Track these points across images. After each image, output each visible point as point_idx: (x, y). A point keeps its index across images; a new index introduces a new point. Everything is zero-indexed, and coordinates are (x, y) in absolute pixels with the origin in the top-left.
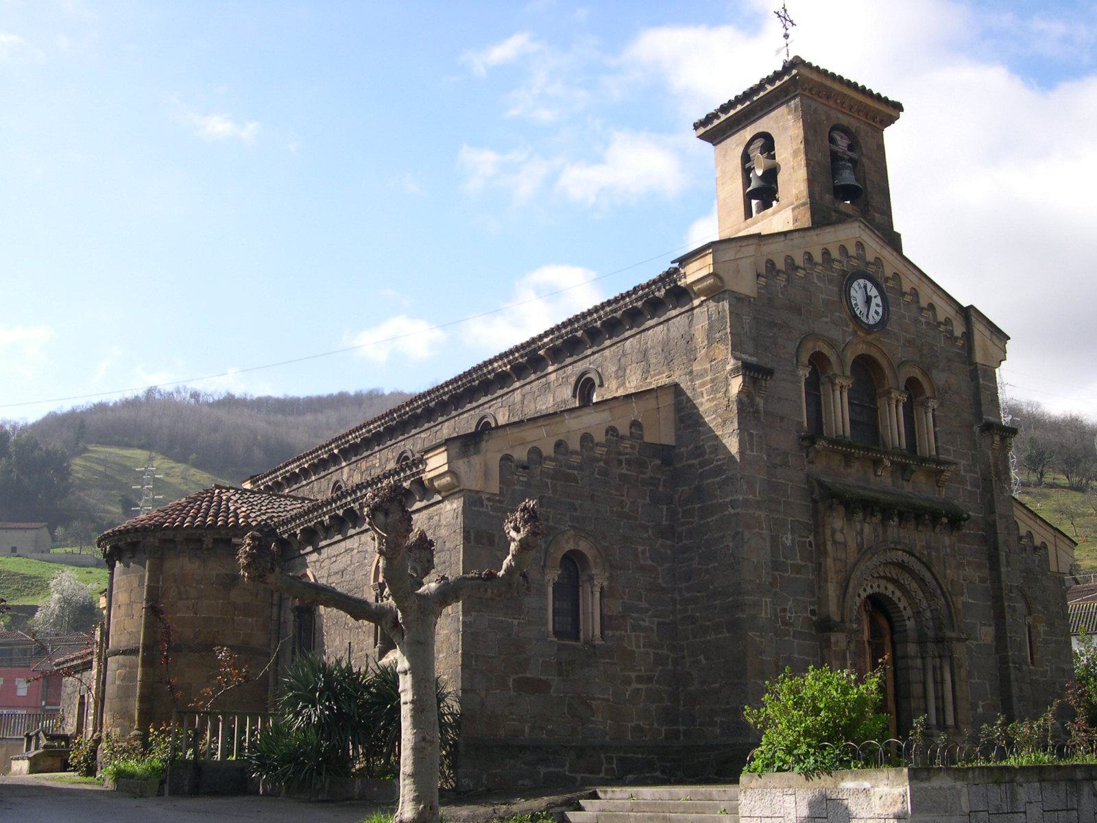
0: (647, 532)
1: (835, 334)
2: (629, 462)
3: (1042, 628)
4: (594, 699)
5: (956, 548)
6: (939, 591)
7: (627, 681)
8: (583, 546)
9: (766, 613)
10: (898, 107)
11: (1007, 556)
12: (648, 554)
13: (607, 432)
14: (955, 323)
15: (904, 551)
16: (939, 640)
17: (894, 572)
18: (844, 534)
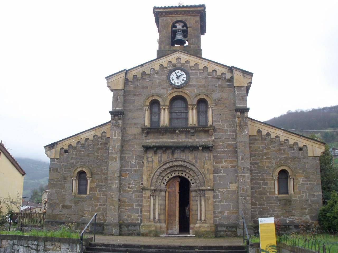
0: (106, 163)
1: (163, 92)
2: (101, 144)
3: (301, 179)
4: (85, 210)
6: (200, 173)
7: (97, 205)
8: (84, 169)
9: (116, 186)
10: (203, 6)
11: (243, 156)
12: (106, 169)
13: (94, 136)
14: (227, 74)
16: (200, 190)
17: (181, 169)
18: (152, 158)
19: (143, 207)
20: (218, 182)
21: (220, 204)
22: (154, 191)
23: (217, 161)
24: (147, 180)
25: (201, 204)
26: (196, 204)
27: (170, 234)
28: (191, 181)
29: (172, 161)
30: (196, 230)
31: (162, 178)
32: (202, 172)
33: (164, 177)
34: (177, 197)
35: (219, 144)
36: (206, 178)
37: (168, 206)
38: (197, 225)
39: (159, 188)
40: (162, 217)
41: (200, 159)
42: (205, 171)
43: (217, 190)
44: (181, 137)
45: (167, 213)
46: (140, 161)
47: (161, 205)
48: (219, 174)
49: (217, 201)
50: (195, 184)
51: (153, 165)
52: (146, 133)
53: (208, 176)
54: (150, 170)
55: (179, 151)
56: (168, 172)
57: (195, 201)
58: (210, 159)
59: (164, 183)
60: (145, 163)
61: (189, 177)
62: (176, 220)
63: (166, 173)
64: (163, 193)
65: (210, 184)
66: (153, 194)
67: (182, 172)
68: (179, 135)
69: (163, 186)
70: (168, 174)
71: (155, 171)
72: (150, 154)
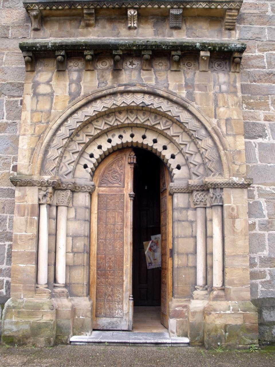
5: (238, 85)
6: (203, 132)
15: (144, 93)
16: (205, 188)
17: (141, 119)
18: (51, 85)
19: (16, 242)
20: (259, 163)
21: (266, 233)
22: (50, 190)
23: (252, 101)
24: (32, 154)
25: (209, 234)
26: (188, 232)
27: (105, 328)
28: (171, 161)
29: (114, 94)
30: (191, 320)
31: (80, 148)
32: (213, 128)
33: (87, 145)
34: (127, 211)
35: (254, 54)
36: (225, 149)
37: (98, 240)
38: (197, 304)
39: (68, 179)
40: (80, 276)
41: (204, 88)
42: (219, 125)
43: (256, 189)
44: (140, 30)
45: (94, 263)
46: (16, 99)
47: (75, 237)
48: (260, 140)
49: (257, 223)
50: (184, 169)
51: (51, 108)
52: (35, 17)
53: (229, 140)
54: (41, 122)
55: (137, 63)
56: (99, 131)
57: (185, 224)
58: (232, 89)
59: (85, 166)
60: (28, 99)
61: (165, 148)
62: (122, 285)
63: (92, 134)
64: (82, 199)
65: (237, 167)
66: (48, 199)
67: (143, 133)
68: (135, 25)
69: (83, 176)
70: (98, 137)
71: (59, 121)
72: (45, 74)
